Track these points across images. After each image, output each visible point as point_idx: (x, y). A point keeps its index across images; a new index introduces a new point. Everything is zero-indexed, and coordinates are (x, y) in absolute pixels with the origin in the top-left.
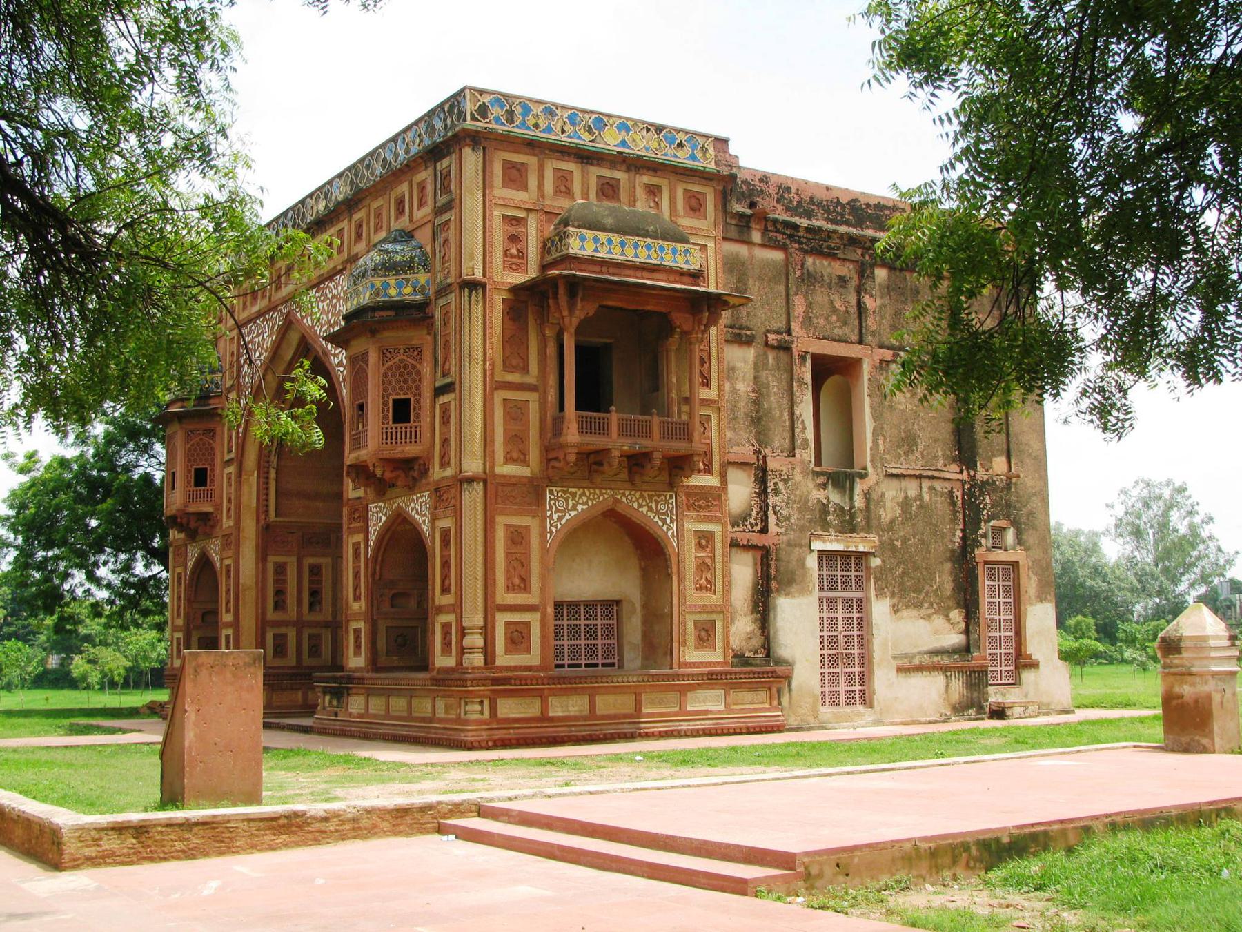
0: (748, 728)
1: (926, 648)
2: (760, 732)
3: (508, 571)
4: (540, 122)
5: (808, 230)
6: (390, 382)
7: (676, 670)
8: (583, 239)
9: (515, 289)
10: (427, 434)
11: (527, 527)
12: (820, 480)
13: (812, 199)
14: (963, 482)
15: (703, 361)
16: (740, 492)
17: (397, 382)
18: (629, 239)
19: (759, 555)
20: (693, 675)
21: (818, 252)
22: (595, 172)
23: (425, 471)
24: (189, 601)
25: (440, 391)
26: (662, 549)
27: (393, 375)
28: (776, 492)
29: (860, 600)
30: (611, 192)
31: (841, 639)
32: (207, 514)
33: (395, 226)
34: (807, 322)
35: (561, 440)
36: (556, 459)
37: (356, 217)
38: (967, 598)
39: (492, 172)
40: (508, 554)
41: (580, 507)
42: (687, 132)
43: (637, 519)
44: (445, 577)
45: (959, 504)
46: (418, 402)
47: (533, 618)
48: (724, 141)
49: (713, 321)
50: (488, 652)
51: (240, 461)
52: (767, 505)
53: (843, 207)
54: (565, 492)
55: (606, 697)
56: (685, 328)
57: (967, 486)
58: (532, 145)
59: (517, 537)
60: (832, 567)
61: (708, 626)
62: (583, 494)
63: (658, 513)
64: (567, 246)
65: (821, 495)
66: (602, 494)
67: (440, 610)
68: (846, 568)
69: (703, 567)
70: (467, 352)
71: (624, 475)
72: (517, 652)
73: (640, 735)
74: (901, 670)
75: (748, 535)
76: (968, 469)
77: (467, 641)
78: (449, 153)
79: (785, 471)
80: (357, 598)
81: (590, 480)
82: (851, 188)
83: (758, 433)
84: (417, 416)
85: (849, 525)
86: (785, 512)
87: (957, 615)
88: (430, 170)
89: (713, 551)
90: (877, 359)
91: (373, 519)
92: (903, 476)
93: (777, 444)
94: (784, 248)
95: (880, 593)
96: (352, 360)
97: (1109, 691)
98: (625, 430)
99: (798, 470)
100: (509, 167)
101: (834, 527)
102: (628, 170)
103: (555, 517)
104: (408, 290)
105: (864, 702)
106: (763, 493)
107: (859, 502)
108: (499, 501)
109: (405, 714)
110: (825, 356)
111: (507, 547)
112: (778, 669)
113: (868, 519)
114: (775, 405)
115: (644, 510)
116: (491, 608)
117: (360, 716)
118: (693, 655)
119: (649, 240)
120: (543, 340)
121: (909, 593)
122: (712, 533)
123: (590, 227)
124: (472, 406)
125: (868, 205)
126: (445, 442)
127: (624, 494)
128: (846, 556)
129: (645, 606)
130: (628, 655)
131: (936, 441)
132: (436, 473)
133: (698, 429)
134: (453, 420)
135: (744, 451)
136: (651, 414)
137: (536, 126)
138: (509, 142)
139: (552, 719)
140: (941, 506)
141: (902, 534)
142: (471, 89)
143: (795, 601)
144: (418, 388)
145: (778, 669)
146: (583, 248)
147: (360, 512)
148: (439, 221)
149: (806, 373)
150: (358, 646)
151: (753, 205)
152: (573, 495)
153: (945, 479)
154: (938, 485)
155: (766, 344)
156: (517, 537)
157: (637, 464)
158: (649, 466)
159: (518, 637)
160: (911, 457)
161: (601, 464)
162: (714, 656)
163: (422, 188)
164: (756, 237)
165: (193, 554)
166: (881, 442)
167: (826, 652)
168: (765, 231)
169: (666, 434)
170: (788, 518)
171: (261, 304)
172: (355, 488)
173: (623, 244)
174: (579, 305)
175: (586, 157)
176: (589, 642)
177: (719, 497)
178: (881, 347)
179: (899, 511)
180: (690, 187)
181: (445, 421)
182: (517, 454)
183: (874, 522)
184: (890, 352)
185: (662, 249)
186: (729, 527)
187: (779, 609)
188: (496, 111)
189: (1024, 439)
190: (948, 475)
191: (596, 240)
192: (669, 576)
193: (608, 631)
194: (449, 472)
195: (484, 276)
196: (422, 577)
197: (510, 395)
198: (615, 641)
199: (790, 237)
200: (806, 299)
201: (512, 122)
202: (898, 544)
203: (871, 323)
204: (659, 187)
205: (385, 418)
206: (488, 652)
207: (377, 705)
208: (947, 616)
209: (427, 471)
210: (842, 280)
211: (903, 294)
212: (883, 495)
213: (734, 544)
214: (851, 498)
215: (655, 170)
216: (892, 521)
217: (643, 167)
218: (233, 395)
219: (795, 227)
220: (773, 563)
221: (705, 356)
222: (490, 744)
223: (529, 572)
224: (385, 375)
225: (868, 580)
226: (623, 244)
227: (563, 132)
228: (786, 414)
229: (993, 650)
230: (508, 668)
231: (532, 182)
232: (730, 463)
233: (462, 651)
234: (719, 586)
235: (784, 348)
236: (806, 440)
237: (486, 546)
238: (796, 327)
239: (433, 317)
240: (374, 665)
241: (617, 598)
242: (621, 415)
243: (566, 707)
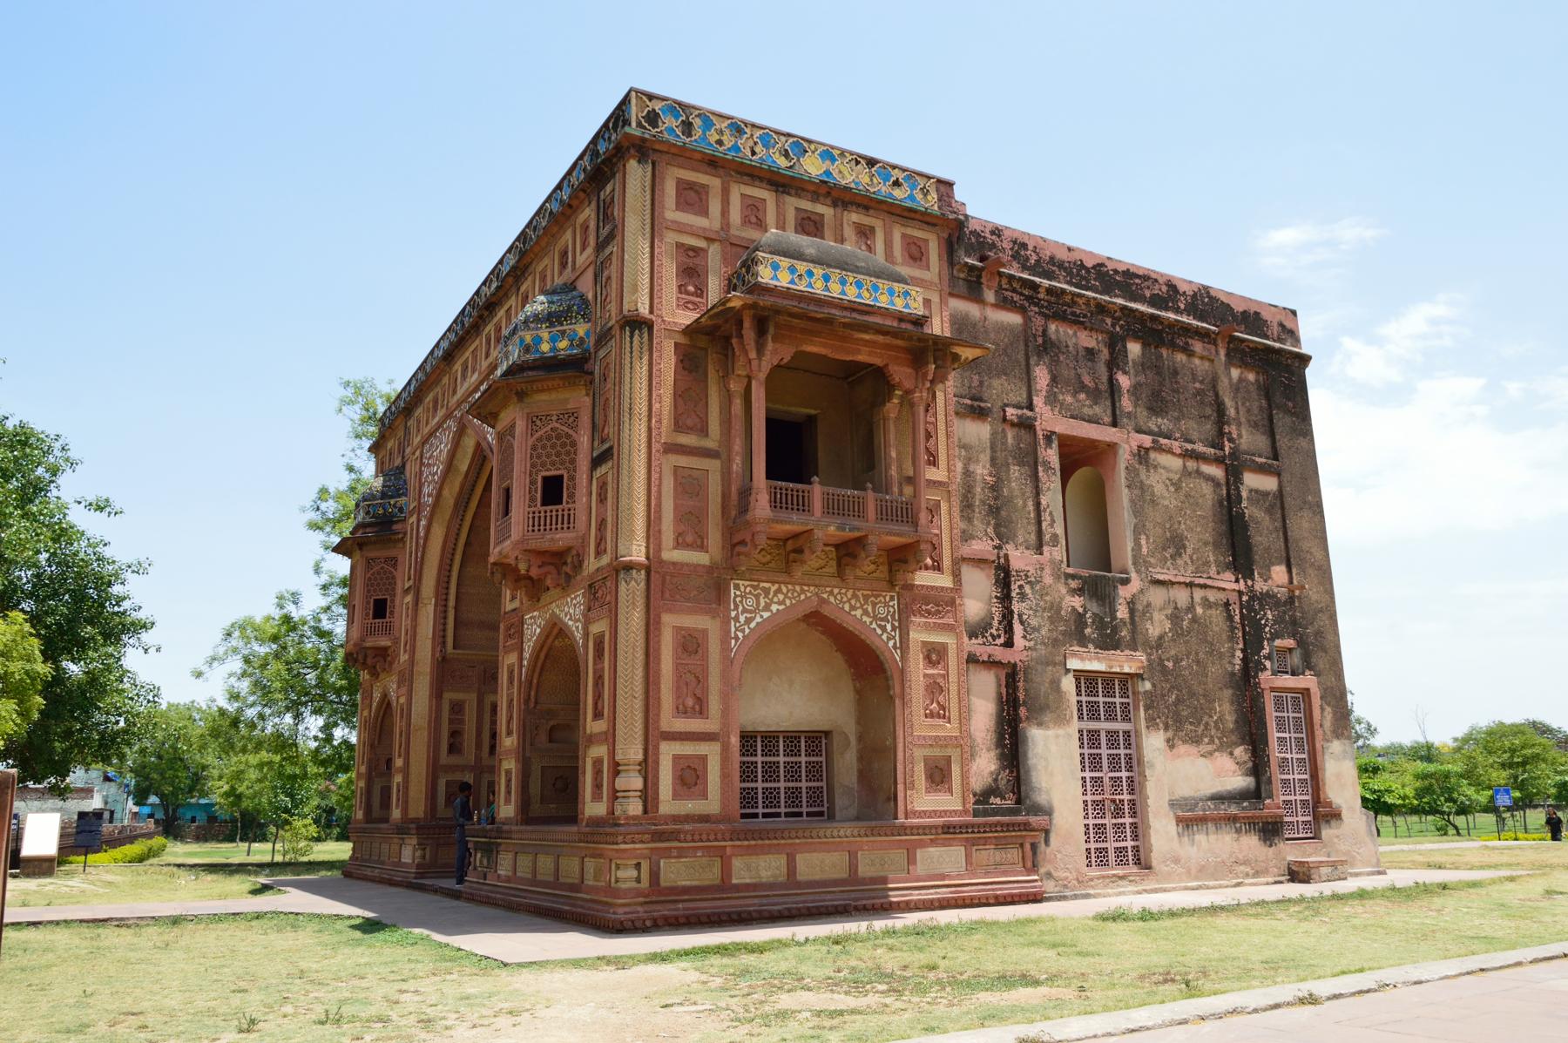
0: (996, 897)
2: (1012, 903)
3: (678, 688)
4: (725, 138)
5: (1050, 291)
6: (539, 457)
7: (901, 820)
8: (776, 267)
9: (689, 331)
10: (581, 518)
11: (705, 632)
12: (1074, 584)
13: (1052, 258)
14: (1240, 593)
15: (928, 436)
16: (977, 597)
17: (548, 456)
18: (835, 274)
20: (924, 828)
21: (1061, 317)
22: (792, 203)
23: (578, 566)
24: (372, 746)
25: (597, 462)
26: (881, 664)
27: (544, 447)
28: (1023, 596)
29: (1127, 733)
30: (812, 228)
31: (1106, 780)
32: (385, 649)
33: (558, 281)
34: (1051, 399)
35: (749, 516)
36: (743, 542)
37: (523, 289)
38: (1252, 734)
39: (663, 190)
40: (678, 667)
41: (774, 608)
42: (904, 170)
43: (849, 624)
44: (598, 697)
45: (1237, 618)
46: (572, 478)
47: (711, 751)
48: (950, 185)
49: (939, 378)
50: (648, 796)
51: (416, 590)
52: (1012, 612)
54: (755, 588)
55: (807, 855)
56: (908, 385)
57: (1245, 598)
58: (713, 163)
59: (691, 644)
60: (1092, 691)
61: (942, 764)
62: (779, 591)
63: (875, 618)
64: (756, 275)
66: (803, 591)
67: (591, 740)
68: (1109, 692)
69: (935, 688)
70: (626, 405)
71: (832, 568)
72: (690, 798)
73: (856, 909)
75: (989, 649)
76: (1244, 578)
77: (620, 783)
78: (613, 175)
79: (1032, 571)
80: (509, 733)
81: (788, 572)
83: (997, 527)
84: (571, 495)
85: (1109, 641)
87: (1239, 751)
88: (594, 204)
89: (946, 668)
90: (1134, 445)
91: (527, 632)
92: (1173, 583)
93: (1021, 539)
94: (1022, 310)
95: (1152, 723)
96: (500, 437)
97: (1419, 847)
98: (833, 508)
99: (1047, 571)
100: (684, 187)
101: (1093, 641)
102: (835, 205)
103: (742, 619)
104: (563, 344)
105: (1138, 862)
106: (1005, 598)
108: (667, 595)
109: (551, 879)
110: (1074, 438)
111: (676, 657)
112: (1032, 819)
113: (1133, 632)
114: (1017, 492)
115: (858, 613)
116: (652, 736)
117: (508, 880)
119: (860, 277)
120: (728, 398)
121: (1184, 723)
122: (944, 647)
123: (786, 254)
124: (631, 471)
125: (1116, 271)
126: (602, 524)
127: (831, 593)
128: (1109, 681)
129: (860, 739)
130: (840, 802)
131: (1206, 544)
132: (592, 564)
133: (923, 517)
134: (610, 495)
135: (982, 546)
136: (865, 489)
137: (720, 142)
138: (683, 155)
139: (738, 888)
141: (1173, 652)
142: (637, 92)
143: (1051, 733)
144: (573, 461)
145: (1032, 819)
146: (775, 277)
147: (517, 630)
148: (601, 258)
149: (1052, 455)
150: (509, 792)
151: (982, 259)
152: (766, 591)
153: (1219, 589)
154: (1212, 596)
155: (1004, 419)
156: (691, 644)
157: (848, 555)
158: (863, 555)
159: (690, 777)
160: (1180, 562)
161: (800, 551)
163: (586, 228)
164: (990, 296)
165: (377, 695)
166: (1143, 542)
167: (1089, 798)
168: (999, 291)
169: (885, 514)
170: (1035, 629)
171: (441, 413)
172: (513, 598)
173: (826, 278)
174: (770, 346)
175: (783, 184)
176: (791, 784)
177: (952, 603)
179: (1168, 625)
180: (909, 231)
181: (602, 499)
182: (691, 535)
183: (1140, 639)
184: (1149, 438)
185: (876, 288)
186: (966, 639)
188: (669, 122)
189: (1305, 545)
190: (1223, 585)
191: (792, 269)
192: (892, 699)
193: (814, 771)
194: (605, 560)
195: (651, 312)
196: (575, 705)
197: (683, 461)
198: (824, 784)
199: (1028, 298)
200: (1051, 372)
201: (690, 135)
202: (1170, 664)
203: (1126, 403)
204: (872, 229)
205: (533, 499)
206: (648, 796)
207: (524, 862)
208: (1231, 754)
209: (581, 563)
210: (1090, 353)
212: (1149, 605)
213: (972, 660)
215: (867, 208)
216: (1161, 637)
217: (852, 203)
218: (413, 519)
219: (1035, 287)
220: (1021, 684)
221: (930, 428)
222: (648, 923)
223: (706, 690)
224: (534, 448)
225: (1136, 708)
226: (826, 278)
227: (754, 153)
228: (1030, 503)
229: (1285, 797)
230: (676, 819)
231: (715, 207)
232: (964, 559)
233: (614, 795)
234: (954, 714)
235: (1026, 425)
236: (1055, 536)
237: (647, 655)
238: (1038, 401)
239: (592, 373)
240: (527, 816)
241: (825, 728)
242: (826, 489)
243: (759, 868)
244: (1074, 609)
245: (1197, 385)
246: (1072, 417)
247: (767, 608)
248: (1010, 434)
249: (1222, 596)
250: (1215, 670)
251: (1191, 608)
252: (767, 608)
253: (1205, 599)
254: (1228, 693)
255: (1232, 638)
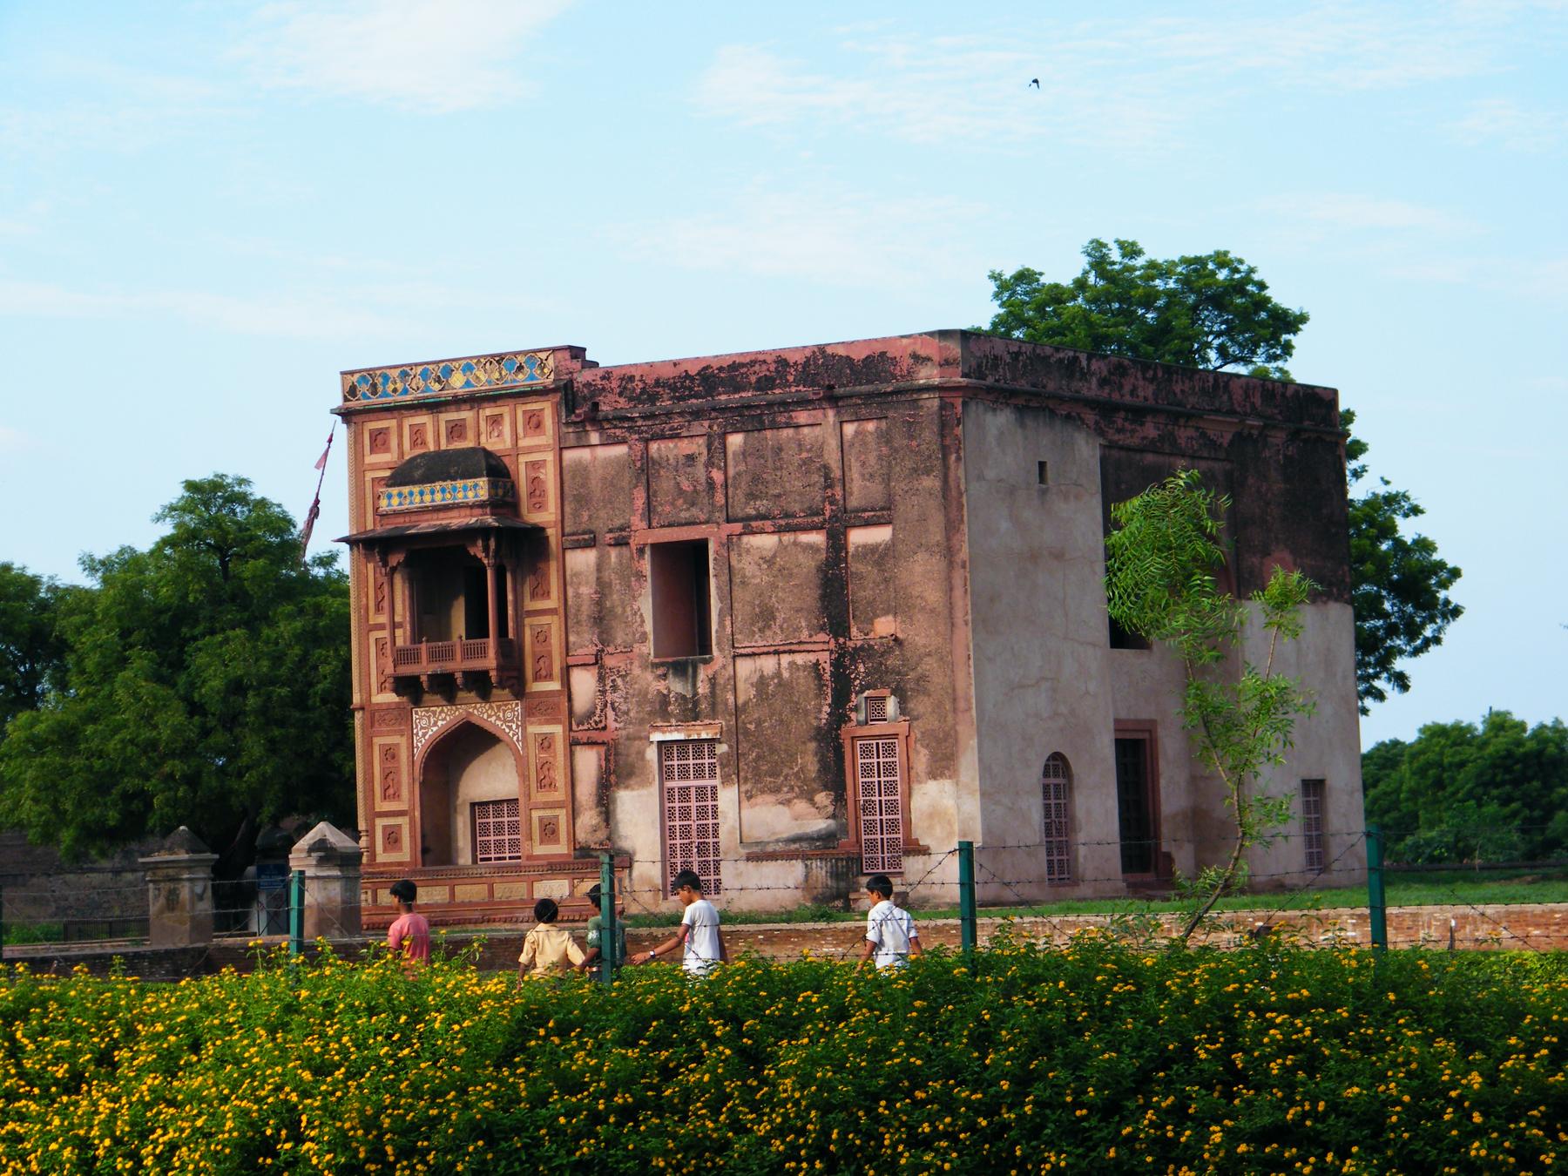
1: (785, 836)
13: (657, 381)
19: (603, 749)
28: (615, 688)
38: (834, 777)
45: (827, 676)
47: (403, 821)
53: (692, 379)
59: (390, 754)
63: (505, 721)
65: (661, 686)
74: (750, 858)
82: (701, 355)
85: (691, 711)
86: (624, 708)
92: (754, 654)
93: (619, 641)
94: (623, 442)
95: (726, 780)
99: (636, 663)
107: (703, 688)
111: (381, 762)
113: (713, 705)
118: (540, 850)
125: (721, 369)
140: (805, 682)
143: (635, 793)
152: (434, 713)
160: (768, 633)
162: (561, 848)
170: (627, 713)
178: (728, 521)
180: (529, 407)
183: (720, 707)
187: (619, 803)
188: (364, 388)
191: (400, 495)
199: (629, 428)
202: (752, 727)
208: (811, 801)
210: (691, 459)
211: (762, 457)
214: (694, 685)
226: (422, 494)
230: (384, 864)
236: (644, 634)
244: (659, 692)
245: (804, 455)
246: (670, 525)
247: (435, 724)
248: (614, 553)
249: (812, 658)
250: (800, 727)
251: (778, 674)
252: (435, 724)
253: (792, 664)
254: (812, 746)
255: (820, 693)
